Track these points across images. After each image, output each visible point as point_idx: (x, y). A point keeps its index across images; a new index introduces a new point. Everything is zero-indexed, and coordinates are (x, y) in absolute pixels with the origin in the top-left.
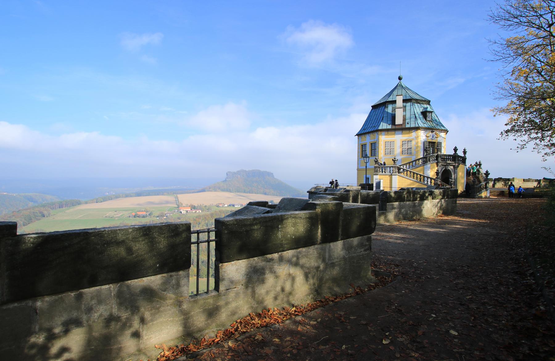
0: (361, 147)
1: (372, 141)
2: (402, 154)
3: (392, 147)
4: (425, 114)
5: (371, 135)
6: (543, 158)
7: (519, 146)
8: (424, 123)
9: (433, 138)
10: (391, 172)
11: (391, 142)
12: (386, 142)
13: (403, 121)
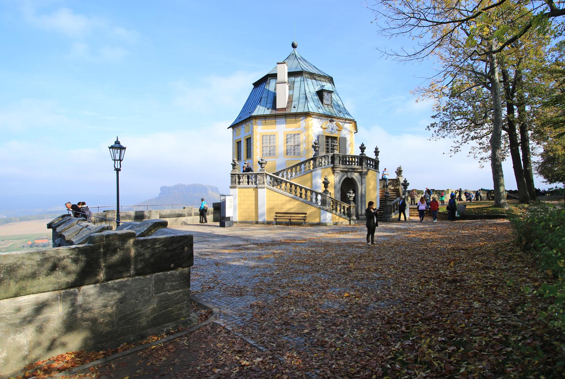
0: (236, 145)
1: (247, 135)
2: (287, 154)
3: (272, 144)
4: (320, 94)
6: (480, 164)
7: (453, 149)
8: (320, 107)
9: (334, 131)
10: (258, 182)
11: (270, 136)
12: (263, 136)
13: (288, 103)
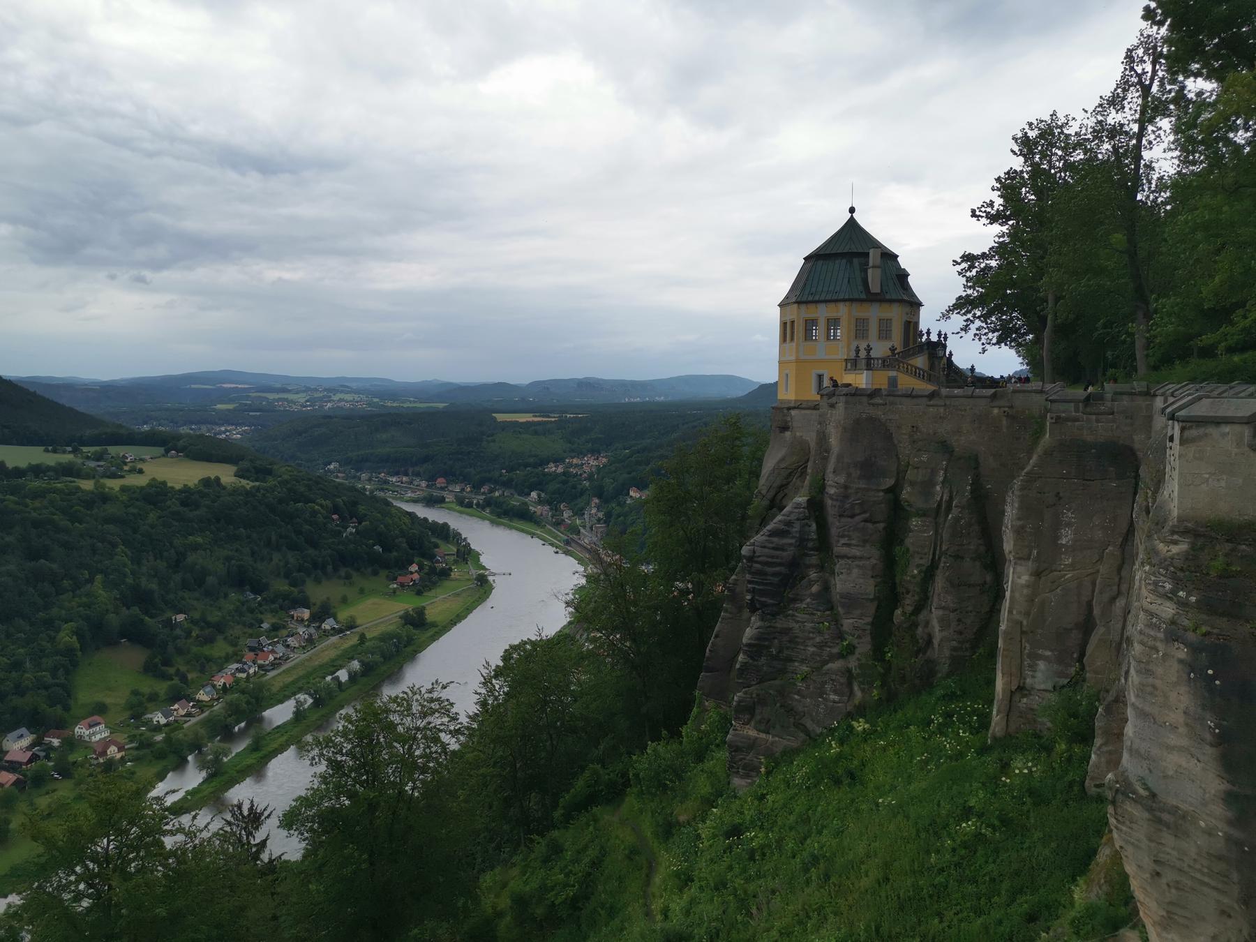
5: (832, 305)
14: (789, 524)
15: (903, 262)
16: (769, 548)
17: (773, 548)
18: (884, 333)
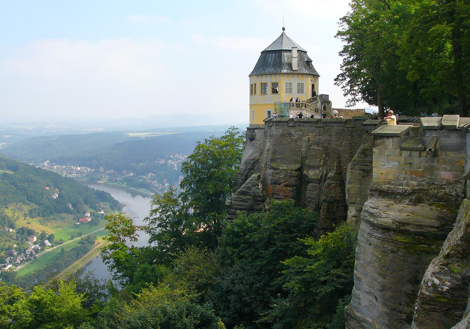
11: (290, 83)
14: (249, 188)
15: (310, 55)
16: (239, 201)
17: (241, 201)
18: (301, 90)
